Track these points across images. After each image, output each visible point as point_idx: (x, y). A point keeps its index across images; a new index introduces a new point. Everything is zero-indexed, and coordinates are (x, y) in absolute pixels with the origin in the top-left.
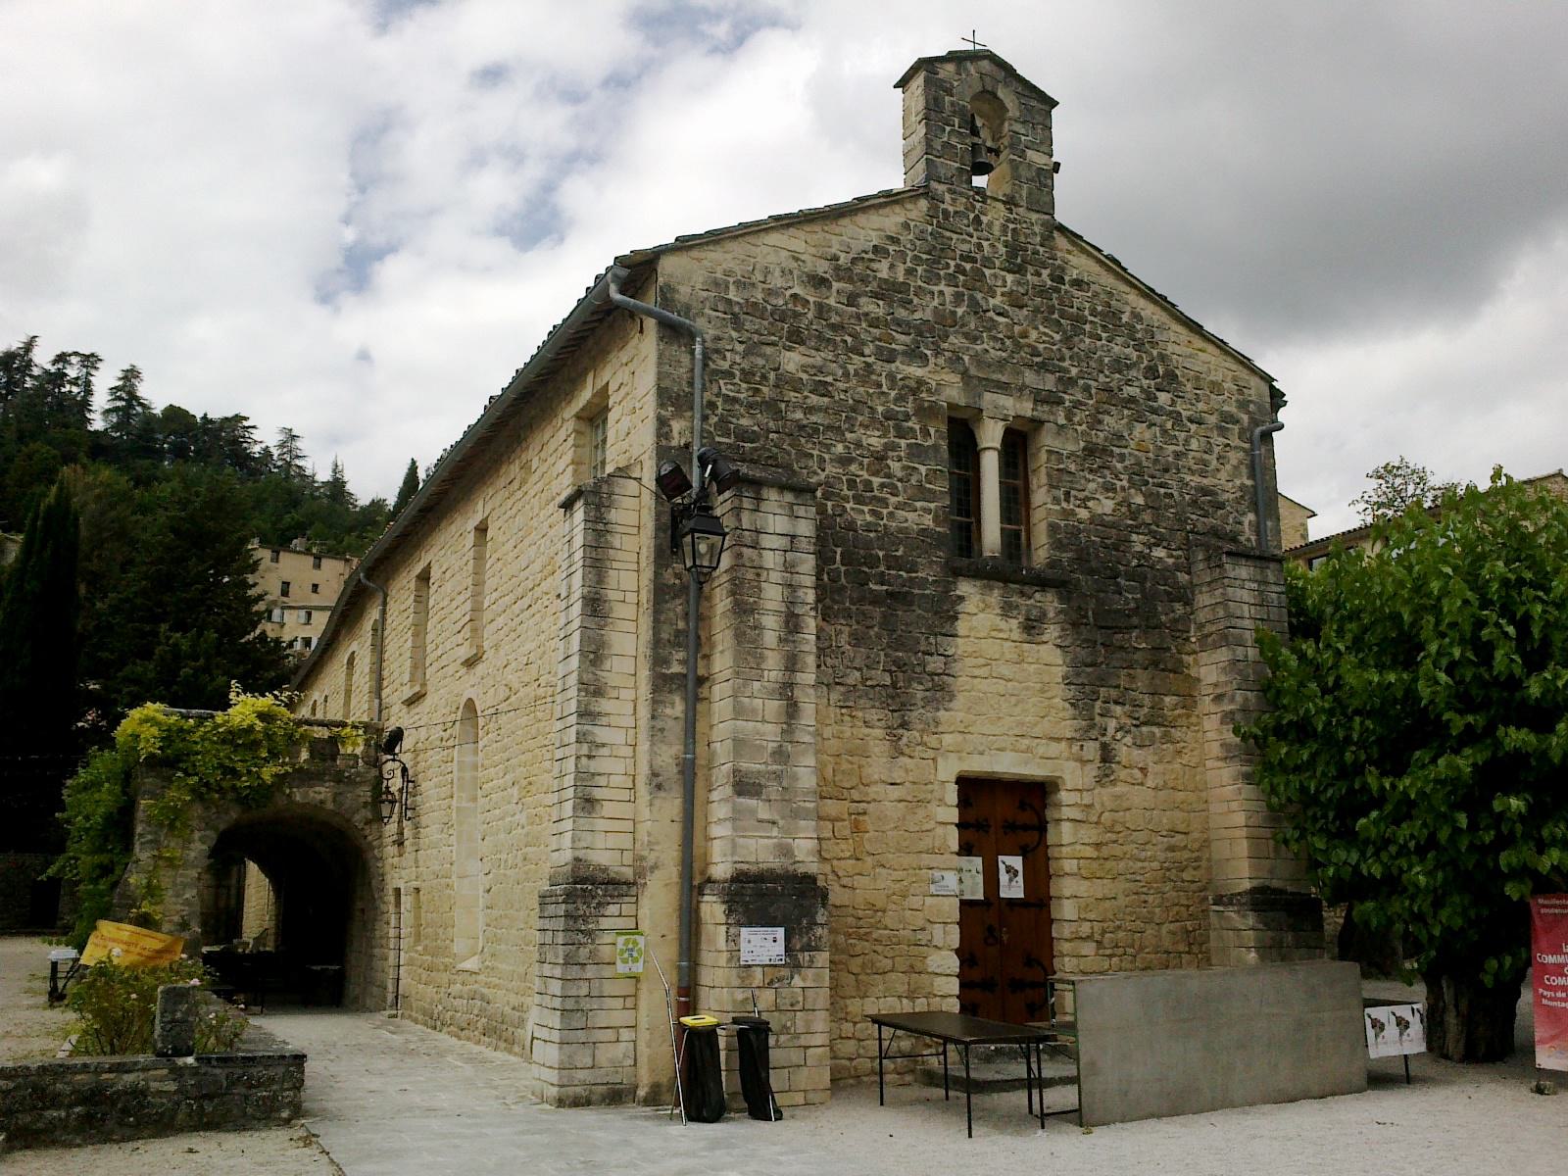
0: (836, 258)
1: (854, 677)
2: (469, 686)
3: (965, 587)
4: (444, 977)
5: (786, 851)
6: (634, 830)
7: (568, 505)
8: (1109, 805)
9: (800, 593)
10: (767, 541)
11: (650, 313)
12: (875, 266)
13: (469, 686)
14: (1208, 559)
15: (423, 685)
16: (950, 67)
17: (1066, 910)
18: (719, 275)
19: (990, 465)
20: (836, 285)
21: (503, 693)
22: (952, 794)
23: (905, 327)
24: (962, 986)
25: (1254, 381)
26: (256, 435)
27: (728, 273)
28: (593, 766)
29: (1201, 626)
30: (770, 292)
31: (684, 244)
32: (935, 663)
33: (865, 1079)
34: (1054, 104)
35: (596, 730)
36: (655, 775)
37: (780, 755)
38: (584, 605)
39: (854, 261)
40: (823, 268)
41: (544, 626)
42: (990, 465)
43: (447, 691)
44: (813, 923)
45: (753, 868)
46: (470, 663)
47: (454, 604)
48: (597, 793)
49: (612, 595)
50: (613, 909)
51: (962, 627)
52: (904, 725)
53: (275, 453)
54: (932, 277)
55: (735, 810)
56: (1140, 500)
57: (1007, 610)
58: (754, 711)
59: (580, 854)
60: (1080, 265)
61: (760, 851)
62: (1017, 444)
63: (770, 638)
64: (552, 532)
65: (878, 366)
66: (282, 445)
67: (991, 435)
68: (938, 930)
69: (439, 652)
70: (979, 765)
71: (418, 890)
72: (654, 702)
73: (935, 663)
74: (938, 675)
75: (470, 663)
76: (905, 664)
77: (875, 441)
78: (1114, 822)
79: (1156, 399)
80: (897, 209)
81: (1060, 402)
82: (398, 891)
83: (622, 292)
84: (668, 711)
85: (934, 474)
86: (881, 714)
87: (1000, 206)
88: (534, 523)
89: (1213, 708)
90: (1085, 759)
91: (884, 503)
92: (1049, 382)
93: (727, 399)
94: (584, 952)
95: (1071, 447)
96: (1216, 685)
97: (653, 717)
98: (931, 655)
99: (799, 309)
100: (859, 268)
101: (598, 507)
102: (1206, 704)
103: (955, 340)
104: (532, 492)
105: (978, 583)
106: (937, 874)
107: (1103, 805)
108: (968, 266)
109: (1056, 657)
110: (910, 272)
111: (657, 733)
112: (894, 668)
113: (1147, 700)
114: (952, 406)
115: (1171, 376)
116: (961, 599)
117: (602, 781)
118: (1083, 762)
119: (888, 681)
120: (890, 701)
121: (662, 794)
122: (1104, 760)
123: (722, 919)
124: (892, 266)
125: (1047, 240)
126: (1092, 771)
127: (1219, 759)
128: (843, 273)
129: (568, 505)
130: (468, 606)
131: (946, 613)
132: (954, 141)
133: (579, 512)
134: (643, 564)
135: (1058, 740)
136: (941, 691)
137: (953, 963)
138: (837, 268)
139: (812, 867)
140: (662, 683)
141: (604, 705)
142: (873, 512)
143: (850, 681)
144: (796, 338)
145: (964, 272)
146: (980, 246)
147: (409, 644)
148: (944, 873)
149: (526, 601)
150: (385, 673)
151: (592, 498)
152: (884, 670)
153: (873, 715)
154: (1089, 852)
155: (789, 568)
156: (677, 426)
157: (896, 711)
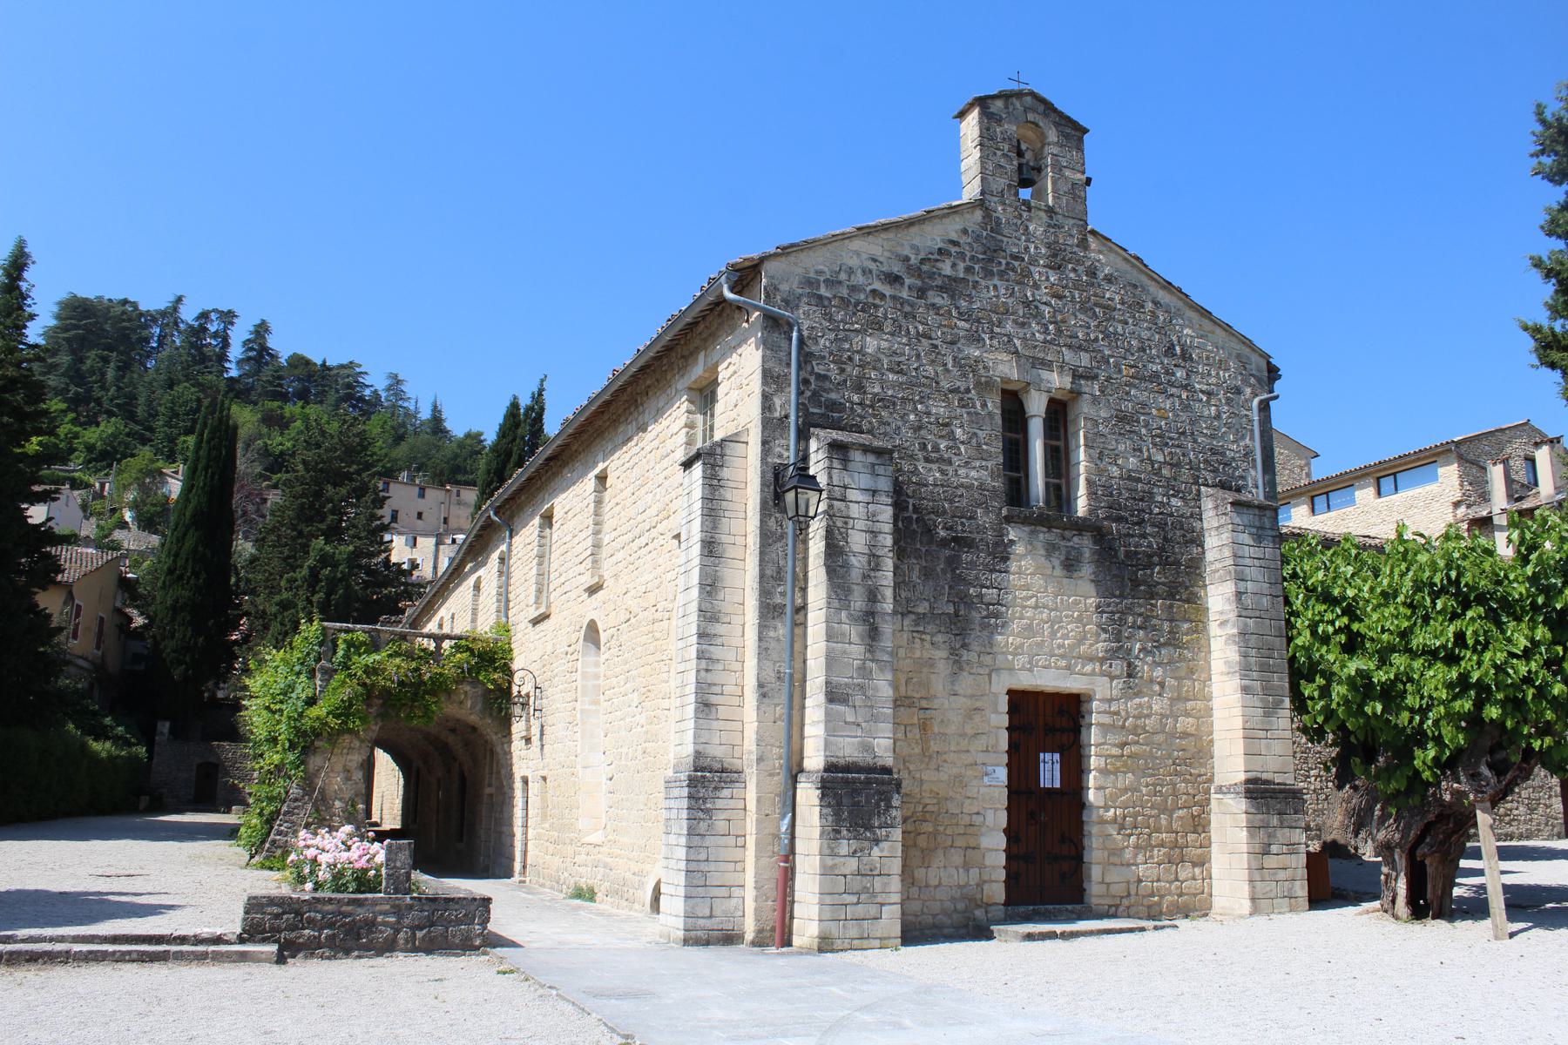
0: (907, 259)
1: (923, 608)
2: (592, 608)
3: (1012, 534)
4: (570, 849)
5: (868, 748)
6: (746, 730)
7: (687, 465)
8: (1133, 712)
9: (880, 537)
10: (853, 495)
11: (757, 308)
12: (939, 265)
13: (592, 608)
14: (1216, 508)
15: (548, 607)
16: (999, 104)
18: (812, 275)
19: (1036, 428)
20: (907, 281)
21: (623, 616)
22: (1004, 705)
23: (965, 315)
24: (1008, 858)
25: (1254, 358)
26: (367, 380)
27: (821, 272)
28: (710, 678)
30: (854, 289)
31: (786, 251)
34: (1085, 131)
35: (712, 648)
36: (760, 685)
37: (863, 671)
38: (703, 547)
39: (922, 261)
40: (897, 268)
41: (660, 561)
42: (1036, 428)
43: (571, 611)
44: (889, 806)
45: (842, 761)
46: (593, 590)
47: (576, 540)
48: (714, 699)
49: (724, 539)
50: (726, 793)
51: (1013, 566)
52: (964, 646)
53: (383, 395)
54: (988, 274)
55: (827, 714)
56: (1160, 458)
57: (1051, 549)
58: (843, 634)
59: (701, 748)
60: (1107, 264)
61: (849, 750)
62: (1059, 414)
63: (855, 575)
64: (667, 483)
65: (943, 349)
66: (388, 389)
67: (1036, 406)
68: (990, 815)
69: (562, 579)
70: (1026, 681)
71: (544, 779)
72: (760, 626)
75: (593, 590)
77: (939, 409)
78: (1136, 727)
79: (1173, 374)
80: (957, 218)
81: (1095, 377)
82: (525, 781)
83: (732, 290)
84: (772, 634)
85: (991, 437)
87: (1042, 214)
88: (651, 474)
91: (950, 463)
92: (1085, 359)
93: (820, 377)
94: (703, 826)
95: (1103, 414)
96: (1221, 613)
97: (760, 639)
99: (877, 301)
100: (925, 268)
101: (713, 466)
102: (1214, 629)
103: (1009, 327)
104: (648, 449)
105: (1026, 529)
108: (1016, 264)
109: (1091, 589)
110: (969, 270)
111: (763, 652)
113: (1166, 626)
114: (1006, 380)
115: (1186, 356)
116: (1012, 542)
117: (717, 689)
118: (1112, 678)
119: (952, 611)
121: (766, 700)
122: (1130, 676)
123: (817, 802)
124: (954, 265)
125: (1083, 243)
128: (916, 271)
129: (687, 465)
130: (589, 542)
131: (1001, 554)
132: (1003, 162)
133: (698, 469)
134: (750, 514)
135: (1091, 659)
136: (994, 617)
137: (1002, 841)
138: (909, 268)
139: (889, 761)
140: (769, 611)
141: (719, 629)
142: (943, 472)
143: (921, 610)
144: (878, 326)
145: (1014, 270)
146: (1027, 248)
147: (534, 571)
149: (643, 541)
150: (511, 596)
151: (709, 458)
153: (939, 638)
154: (1115, 751)
155: (871, 517)
156: (778, 401)
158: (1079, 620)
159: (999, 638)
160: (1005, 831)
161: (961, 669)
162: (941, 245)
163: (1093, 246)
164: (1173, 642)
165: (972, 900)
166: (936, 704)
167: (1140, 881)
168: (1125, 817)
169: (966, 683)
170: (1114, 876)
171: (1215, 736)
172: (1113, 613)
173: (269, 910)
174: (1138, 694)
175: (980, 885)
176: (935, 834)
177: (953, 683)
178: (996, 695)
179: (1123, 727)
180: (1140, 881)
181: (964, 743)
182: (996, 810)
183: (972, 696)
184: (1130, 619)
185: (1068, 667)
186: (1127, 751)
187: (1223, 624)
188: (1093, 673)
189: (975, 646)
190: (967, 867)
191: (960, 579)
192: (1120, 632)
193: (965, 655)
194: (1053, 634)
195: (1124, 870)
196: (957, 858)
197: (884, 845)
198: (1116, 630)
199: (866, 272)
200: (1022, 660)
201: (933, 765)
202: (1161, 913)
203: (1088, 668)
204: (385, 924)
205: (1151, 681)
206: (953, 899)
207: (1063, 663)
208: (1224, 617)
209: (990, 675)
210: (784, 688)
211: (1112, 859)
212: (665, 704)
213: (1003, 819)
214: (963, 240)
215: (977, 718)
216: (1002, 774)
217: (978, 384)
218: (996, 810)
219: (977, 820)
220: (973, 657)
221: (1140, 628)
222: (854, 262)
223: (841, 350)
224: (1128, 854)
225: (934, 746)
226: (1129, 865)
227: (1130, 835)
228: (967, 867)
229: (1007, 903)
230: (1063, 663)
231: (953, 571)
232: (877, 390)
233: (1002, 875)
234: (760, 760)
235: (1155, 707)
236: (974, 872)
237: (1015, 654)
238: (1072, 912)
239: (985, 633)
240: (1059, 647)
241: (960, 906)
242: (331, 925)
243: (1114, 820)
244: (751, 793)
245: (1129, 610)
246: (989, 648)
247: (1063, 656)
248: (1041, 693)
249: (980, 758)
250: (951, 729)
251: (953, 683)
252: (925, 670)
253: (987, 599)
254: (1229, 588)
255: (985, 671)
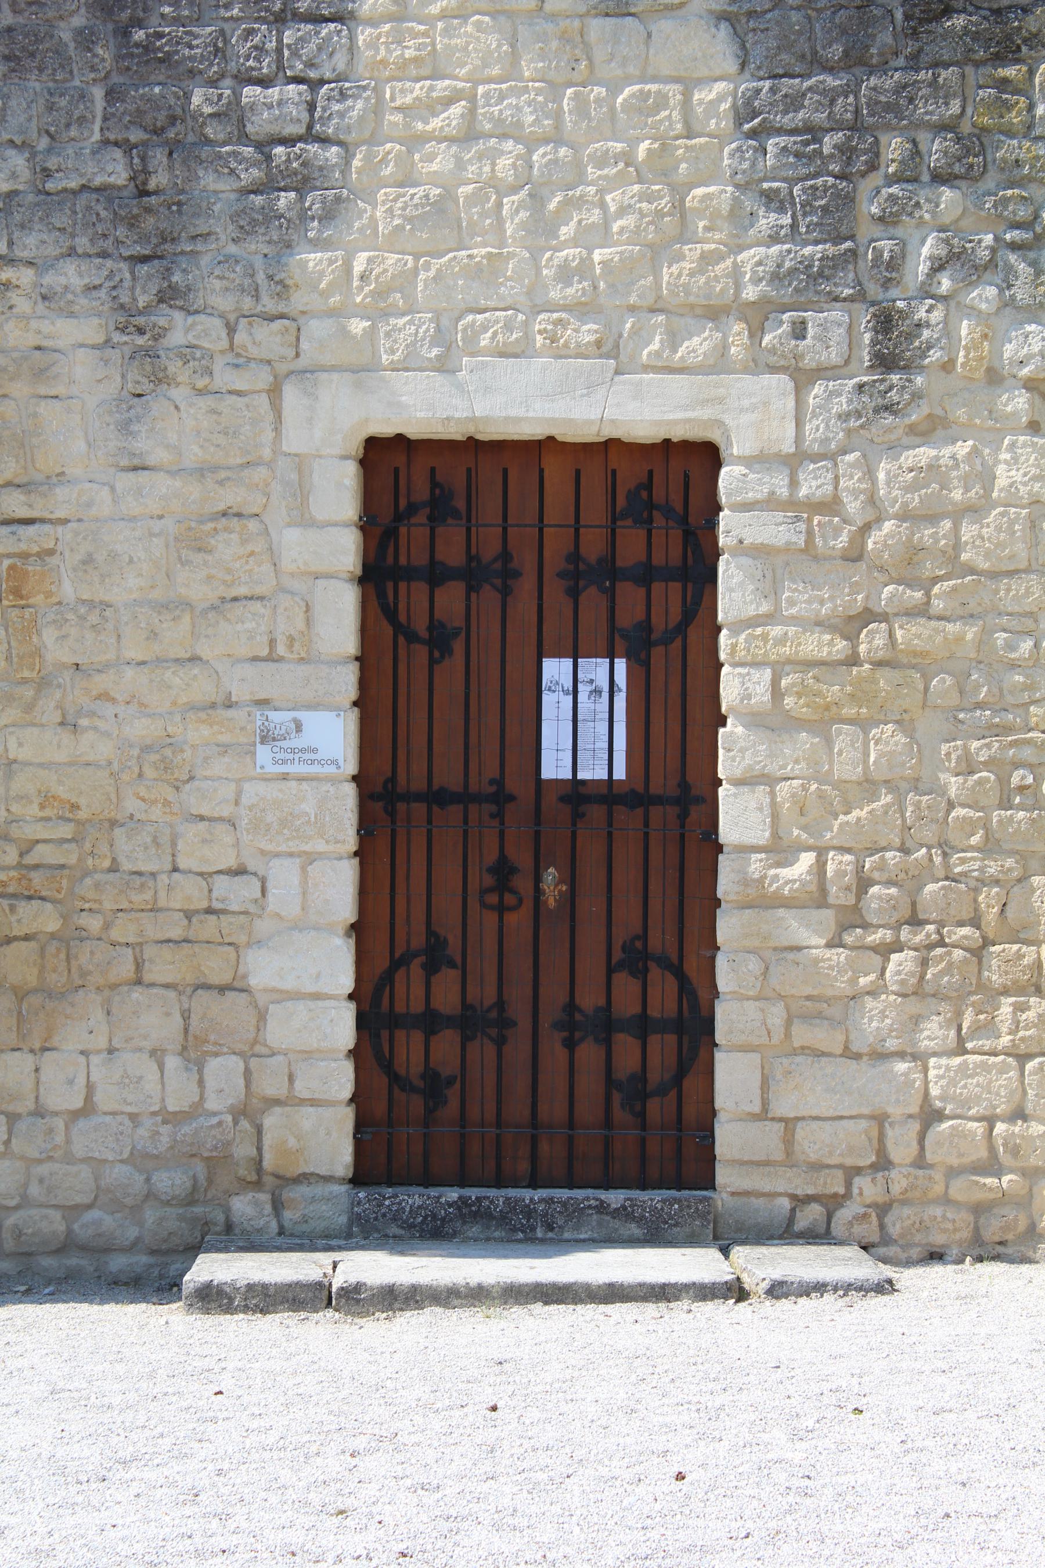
17: (738, 816)
22: (339, 493)
24: (362, 1022)
32: (275, 106)
33: (47, 1262)
68: (284, 877)
70: (428, 407)
73: (275, 106)
74: (288, 141)
76: (173, 120)
78: (913, 553)
86: (93, 272)
90: (808, 362)
98: (265, 82)
106: (279, 718)
107: (872, 499)
109: (718, 49)
112: (136, 135)
118: (803, 378)
119: (116, 171)
120: (121, 232)
122: (884, 362)
126: (832, 400)
135: (714, 314)
136: (294, 185)
148: (303, 715)
152: (106, 142)
153: (71, 275)
157: (144, 259)
158: (660, 166)
159: (313, 259)
161: (160, 379)
165: (217, 1161)
166: (62, 502)
167: (930, 1116)
168: (863, 883)
169: (181, 424)
170: (806, 1093)
172: (813, 132)
174: (926, 431)
175: (249, 1111)
176: (69, 939)
177: (125, 428)
178: (301, 463)
179: (854, 555)
180: (930, 1116)
181: (175, 635)
182: (310, 858)
183: (201, 472)
184: (894, 148)
185: (607, 348)
186: (872, 641)
188: (718, 363)
190: (194, 1049)
191: (154, 58)
192: (848, 200)
193: (179, 330)
194: (542, 229)
195: (862, 1074)
196: (156, 1020)
198: (828, 198)
200: (407, 330)
201: (48, 711)
202: (1032, 1233)
203: (698, 345)
205: (994, 377)
206: (139, 1159)
207: (587, 332)
209: (275, 392)
211: (803, 1035)
213: (338, 890)
215: (227, 547)
216: (333, 738)
218: (310, 858)
219: (236, 893)
220: (208, 333)
221: (939, 178)
224: (876, 1019)
225: (56, 647)
226: (880, 1056)
227: (886, 950)
228: (194, 1049)
229: (359, 1179)
230: (587, 332)
231: (124, 32)
233: (342, 1080)
235: (1003, 476)
236: (224, 1075)
237: (379, 312)
238: (623, 1213)
239: (256, 247)
240: (565, 274)
241: (171, 1181)
243: (817, 895)
245: (894, 110)
246: (272, 295)
247: (583, 309)
248: (548, 445)
249: (243, 682)
250: (125, 588)
251: (125, 428)
252: (19, 389)
253: (259, 125)
255: (263, 378)
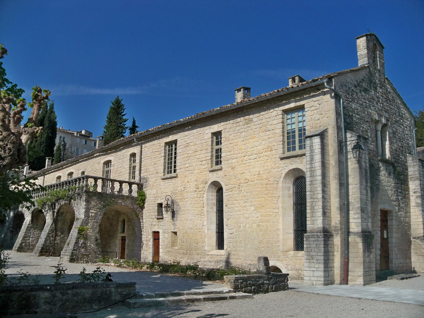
5: (367, 225)
19: (379, 133)
27: (343, 82)
29: (410, 175)
30: (349, 88)
39: (360, 82)
40: (356, 83)
42: (379, 133)
55: (361, 216)
67: (379, 127)
71: (175, 233)
89: (414, 194)
94: (326, 249)
96: (415, 189)
102: (411, 193)
110: (367, 86)
127: (415, 206)
139: (371, 230)
160: (380, 250)
162: (363, 78)
163: (386, 82)
164: (404, 197)
171: (412, 223)
173: (239, 281)
187: (414, 192)
189: (375, 197)
197: (373, 254)
199: (351, 84)
204: (266, 284)
208: (415, 191)
210: (345, 208)
212: (277, 211)
214: (366, 77)
217: (371, 120)
222: (349, 80)
223: (348, 106)
232: (355, 120)
234: (341, 229)
242: (254, 285)
244: (337, 240)
254: (418, 182)
